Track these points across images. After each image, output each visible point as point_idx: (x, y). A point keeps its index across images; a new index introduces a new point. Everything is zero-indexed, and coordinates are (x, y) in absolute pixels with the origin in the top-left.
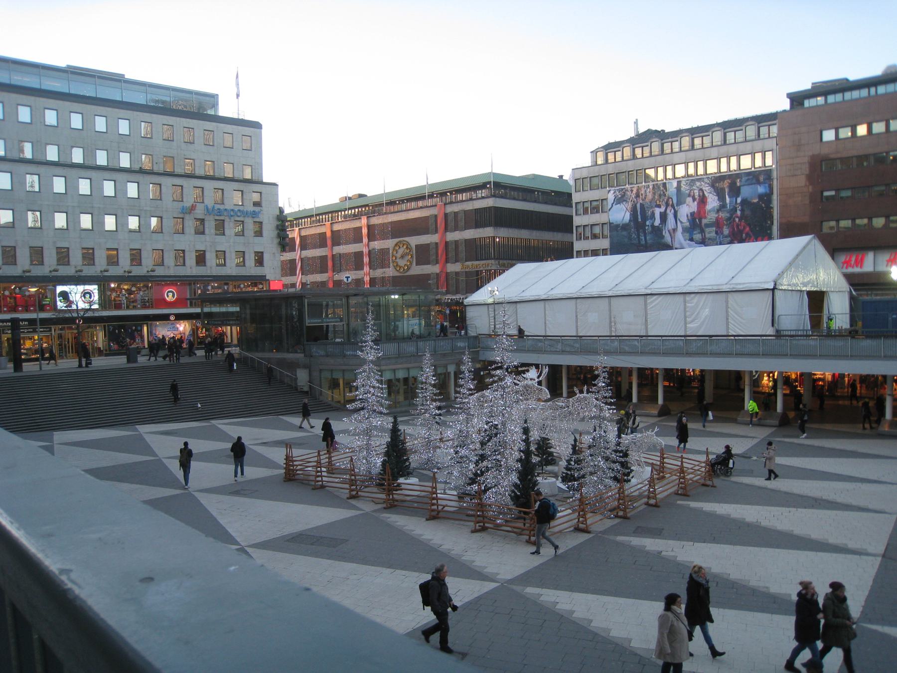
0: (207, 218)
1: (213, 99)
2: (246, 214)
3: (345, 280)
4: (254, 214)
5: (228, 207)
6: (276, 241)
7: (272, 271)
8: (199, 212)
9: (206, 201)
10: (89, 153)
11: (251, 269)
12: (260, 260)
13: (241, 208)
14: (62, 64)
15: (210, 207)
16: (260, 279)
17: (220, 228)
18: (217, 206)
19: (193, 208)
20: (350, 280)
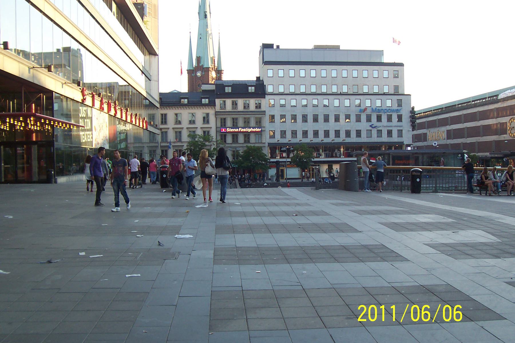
0: (372, 114)
1: (381, 53)
2: (393, 111)
3: (434, 145)
4: (397, 111)
5: (383, 108)
6: (410, 124)
7: (407, 138)
8: (368, 112)
9: (372, 107)
10: (318, 86)
11: (395, 138)
12: (400, 133)
13: (390, 108)
14: (311, 47)
15: (374, 108)
16: (400, 145)
17: (379, 119)
18: (378, 108)
19: (365, 109)
20: (436, 145)
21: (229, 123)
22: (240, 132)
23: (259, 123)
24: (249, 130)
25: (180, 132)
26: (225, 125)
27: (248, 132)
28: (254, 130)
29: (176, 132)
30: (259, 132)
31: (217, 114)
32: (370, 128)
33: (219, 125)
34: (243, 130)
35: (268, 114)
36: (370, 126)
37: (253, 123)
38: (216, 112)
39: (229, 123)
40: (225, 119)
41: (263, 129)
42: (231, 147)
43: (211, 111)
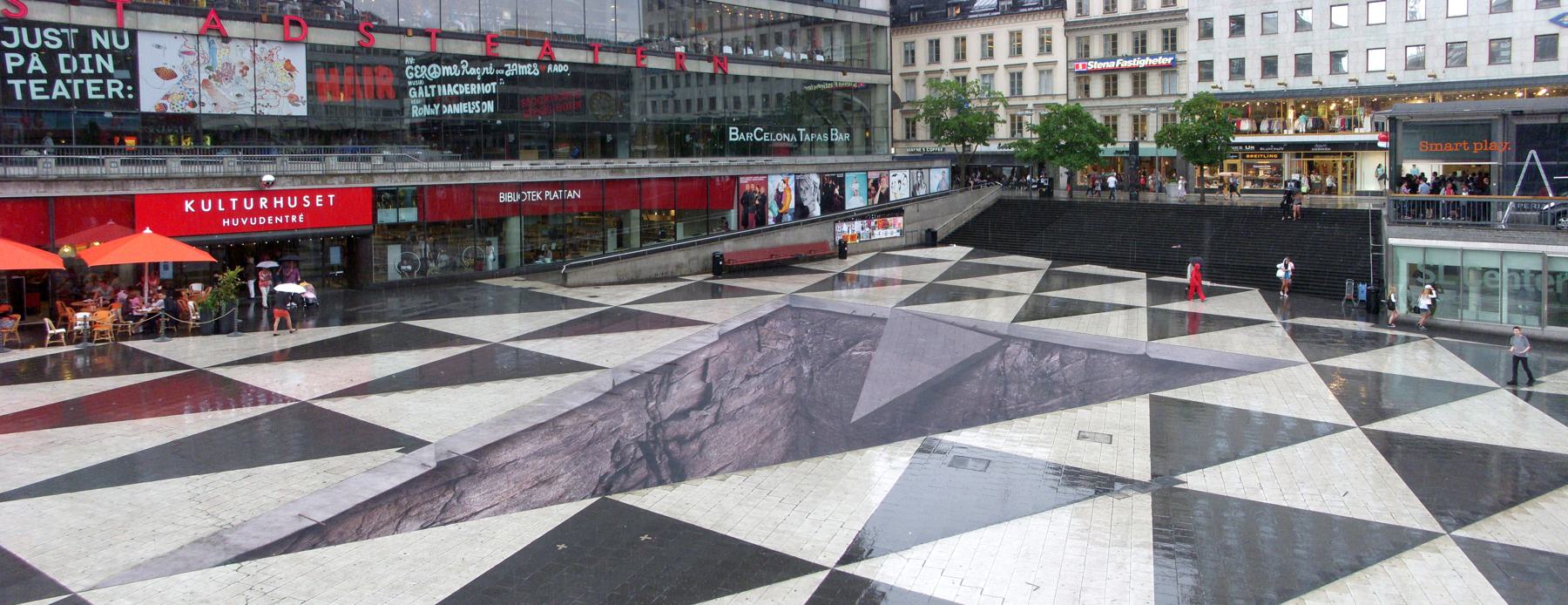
21: (1097, 49)
22: (1120, 69)
23: (1170, 40)
24: (1142, 63)
25: (1020, 75)
26: (1087, 55)
27: (1137, 68)
28: (1153, 62)
29: (1012, 75)
30: (1167, 66)
31: (1069, 27)
32: (1553, 29)
33: (1073, 56)
34: (1126, 64)
35: (1194, 16)
36: (1555, 20)
37: (1154, 43)
38: (1066, 24)
39: (1097, 49)
40: (1144, 35)
41: (1180, 58)
42: (1129, 107)
43: (1056, 24)
